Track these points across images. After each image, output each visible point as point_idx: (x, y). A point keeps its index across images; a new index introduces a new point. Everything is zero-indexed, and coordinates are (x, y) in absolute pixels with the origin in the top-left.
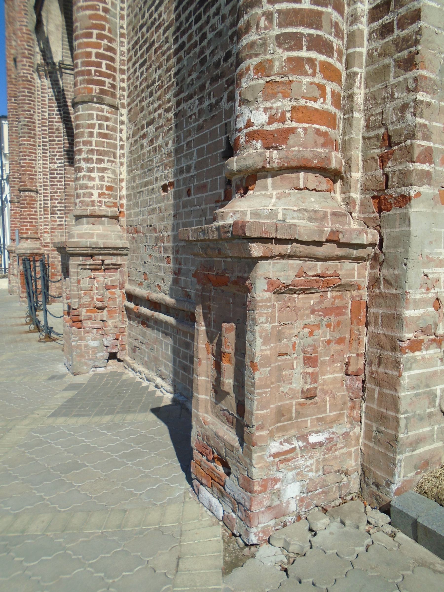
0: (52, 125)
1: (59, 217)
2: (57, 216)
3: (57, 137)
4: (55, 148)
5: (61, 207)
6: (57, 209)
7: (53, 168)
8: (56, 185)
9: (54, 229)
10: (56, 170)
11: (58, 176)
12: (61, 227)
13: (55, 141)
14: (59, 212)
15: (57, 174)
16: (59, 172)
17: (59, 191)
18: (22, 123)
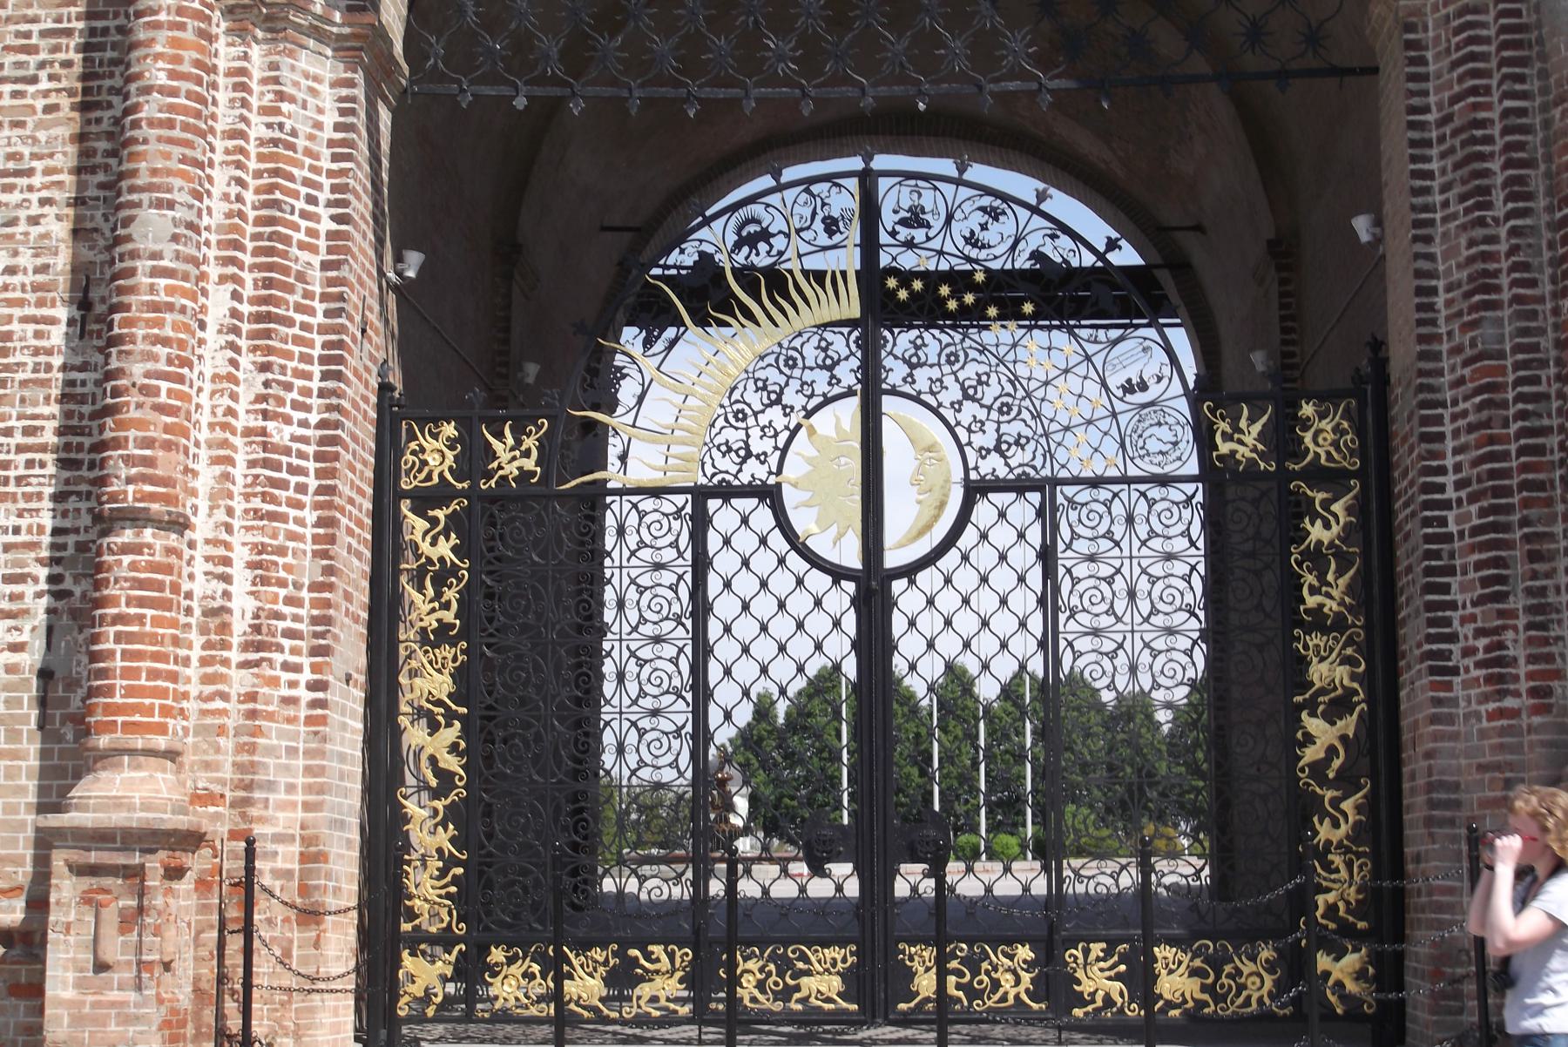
0: (284, 255)
1: (286, 667)
2: (278, 658)
3: (299, 308)
4: (288, 355)
5: (296, 618)
6: (281, 625)
7: (276, 439)
8: (283, 518)
9: (270, 716)
10: (287, 451)
11: (294, 480)
12: (290, 711)
13: (289, 322)
14: (287, 643)
15: (294, 470)
16: (295, 461)
17: (291, 544)
18: (179, 213)
